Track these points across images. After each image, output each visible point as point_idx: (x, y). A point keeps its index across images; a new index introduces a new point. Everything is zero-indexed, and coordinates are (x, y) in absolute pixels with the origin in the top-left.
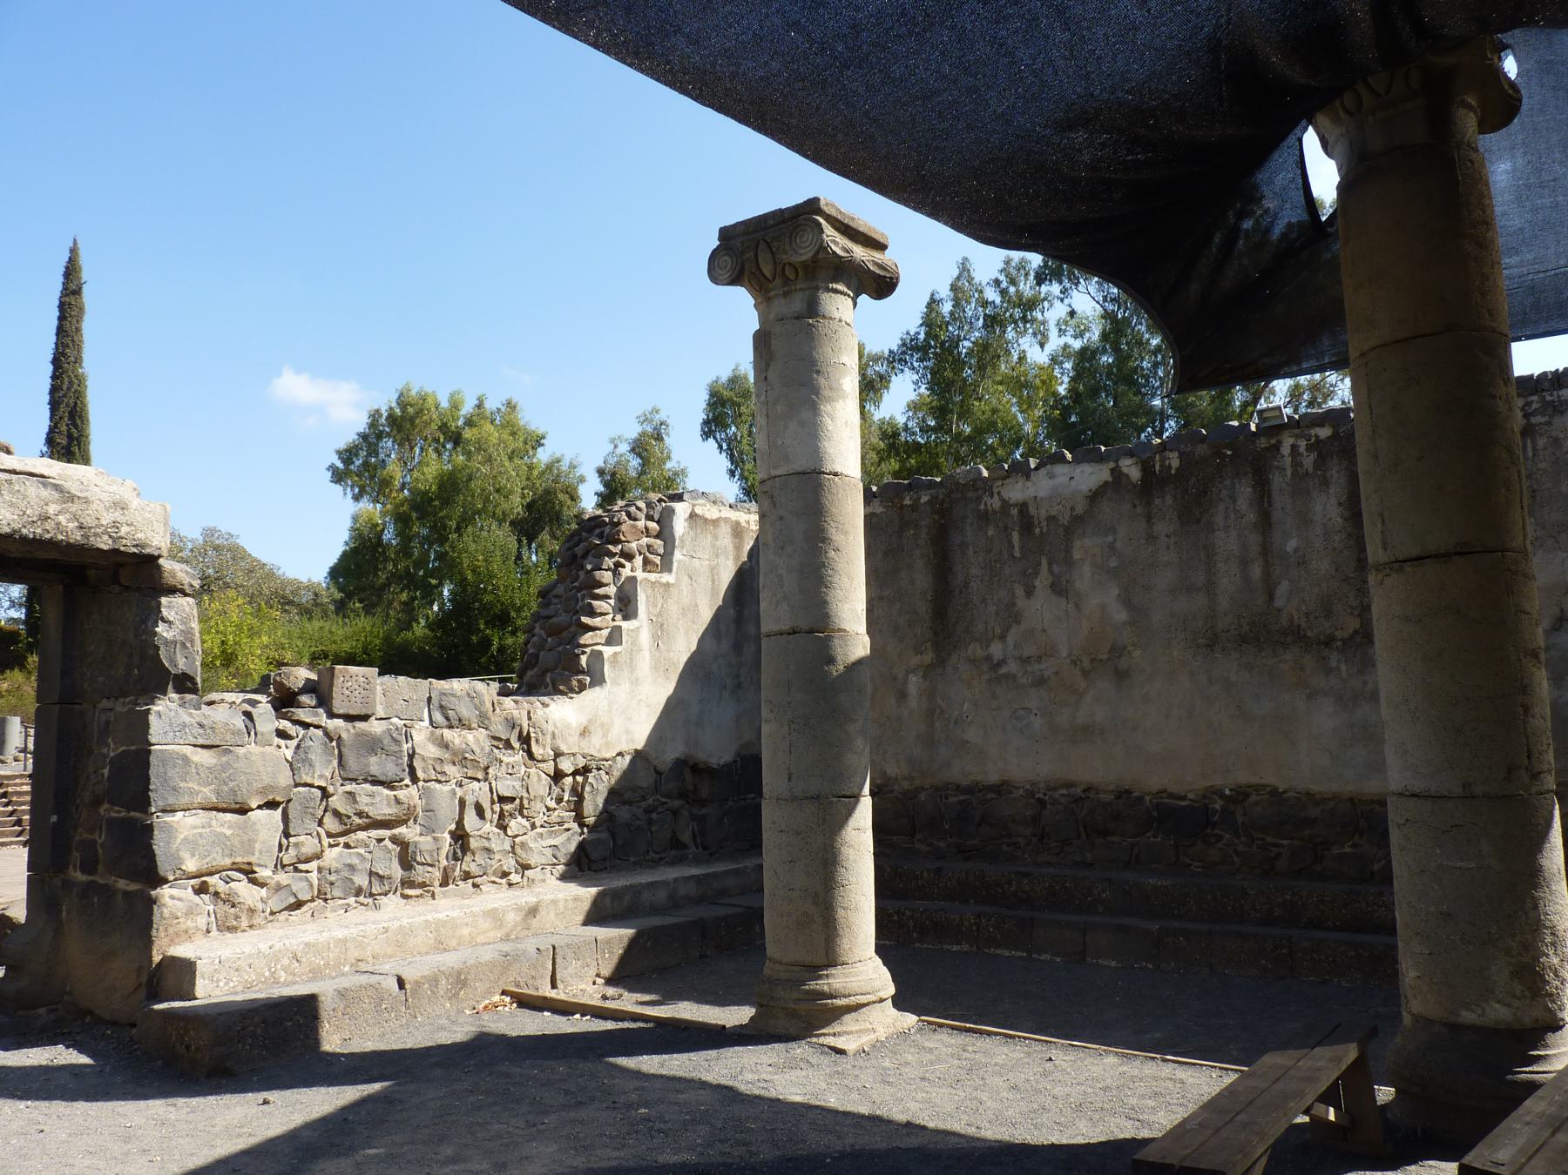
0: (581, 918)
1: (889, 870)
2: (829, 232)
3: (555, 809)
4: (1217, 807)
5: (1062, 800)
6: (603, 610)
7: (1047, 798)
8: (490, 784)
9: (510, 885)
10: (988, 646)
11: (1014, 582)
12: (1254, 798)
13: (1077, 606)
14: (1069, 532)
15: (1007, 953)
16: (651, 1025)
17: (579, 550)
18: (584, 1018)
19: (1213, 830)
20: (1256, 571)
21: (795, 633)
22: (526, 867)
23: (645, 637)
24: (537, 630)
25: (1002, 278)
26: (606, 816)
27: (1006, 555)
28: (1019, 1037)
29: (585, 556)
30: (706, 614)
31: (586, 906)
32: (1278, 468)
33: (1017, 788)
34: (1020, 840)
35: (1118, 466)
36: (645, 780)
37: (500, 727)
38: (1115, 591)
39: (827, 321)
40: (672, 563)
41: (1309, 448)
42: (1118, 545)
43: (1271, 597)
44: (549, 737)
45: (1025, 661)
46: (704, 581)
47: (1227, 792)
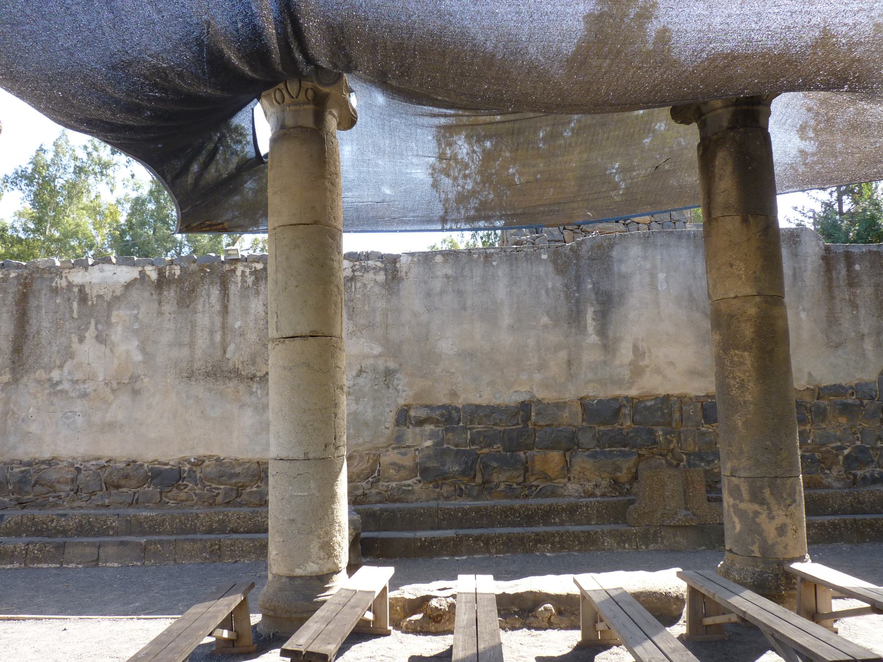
4: (186, 468)
5: (92, 468)
7: (82, 467)
10: (50, 372)
11: (72, 333)
12: (207, 463)
13: (112, 350)
14: (109, 304)
15: (45, 566)
19: (183, 482)
20: (218, 337)
27: (67, 316)
28: (45, 619)
32: (234, 282)
33: (63, 461)
34: (62, 494)
35: (144, 270)
38: (136, 343)
41: (251, 273)
42: (140, 316)
43: (225, 352)
47: (192, 460)
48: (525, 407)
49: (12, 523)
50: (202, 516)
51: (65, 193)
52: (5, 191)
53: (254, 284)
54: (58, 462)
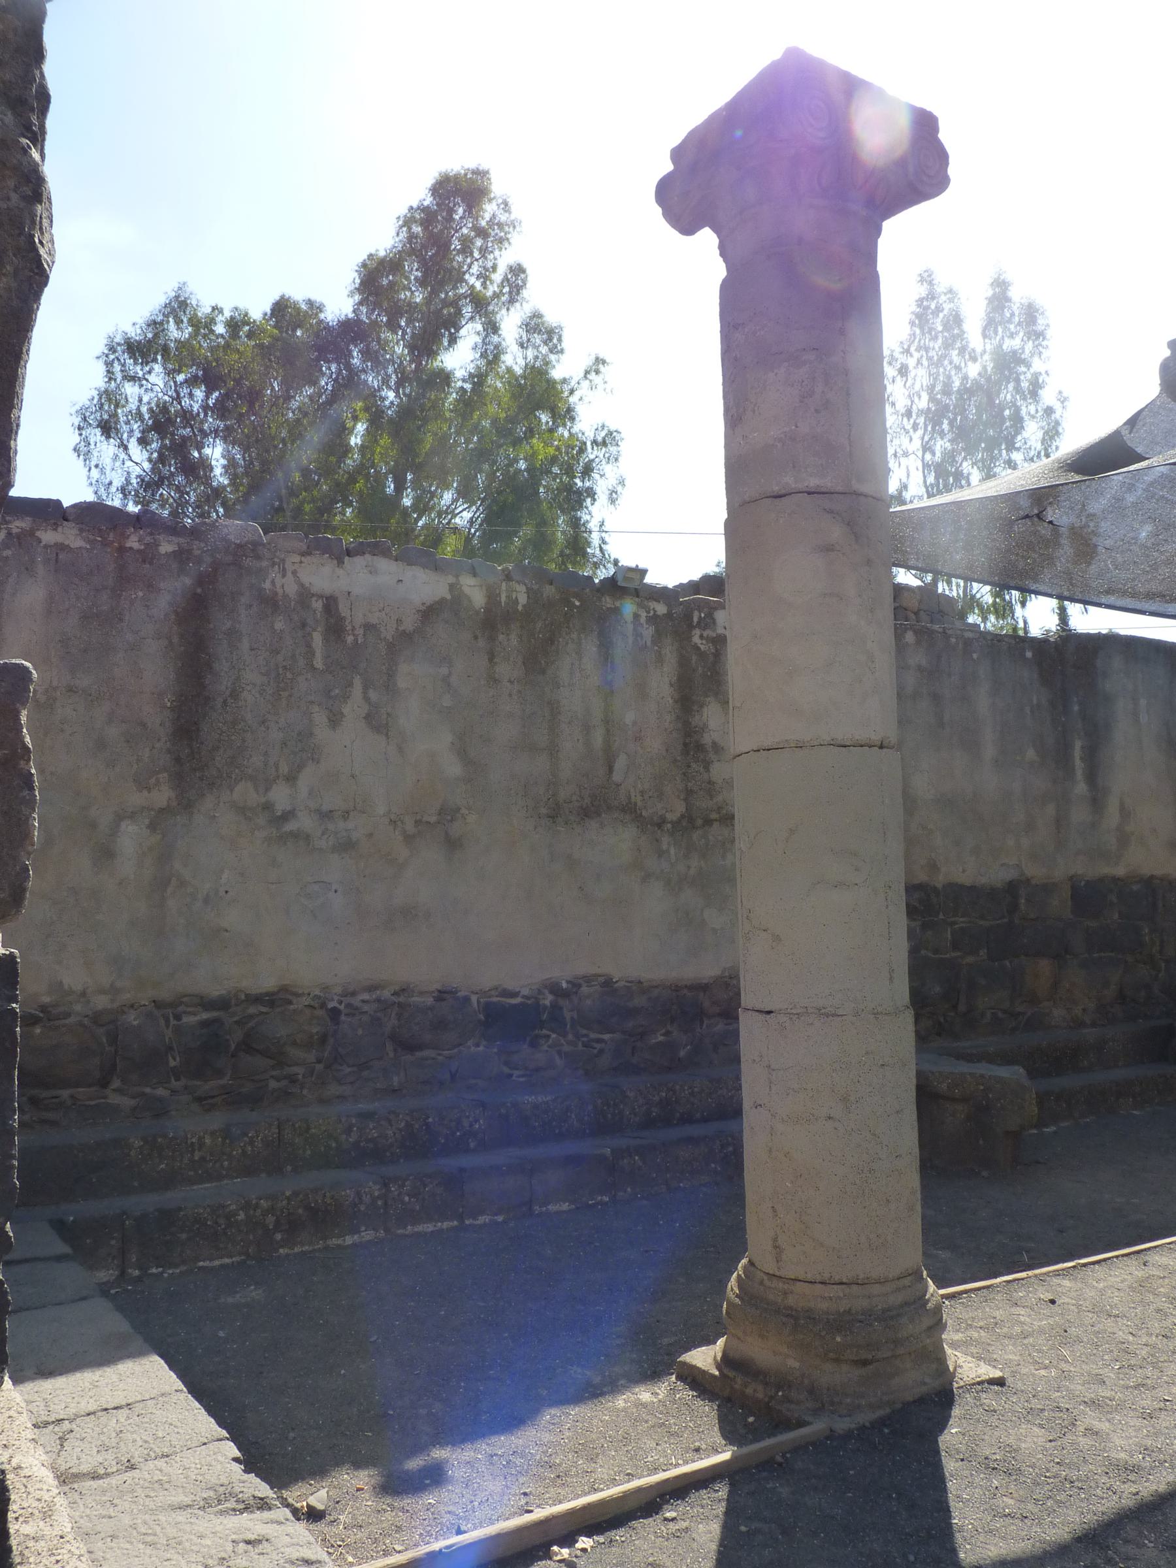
1: (138, 1143)
4: (547, 1002)
5: (366, 1008)
7: (342, 1007)
10: (267, 790)
11: (312, 702)
12: (585, 989)
13: (400, 750)
14: (393, 649)
15: (429, 1227)
27: (301, 662)
34: (295, 1069)
43: (611, 769)
45: (326, 816)
47: (564, 985)
48: (1012, 887)
49: (259, 1144)
53: (654, 642)
54: (290, 997)
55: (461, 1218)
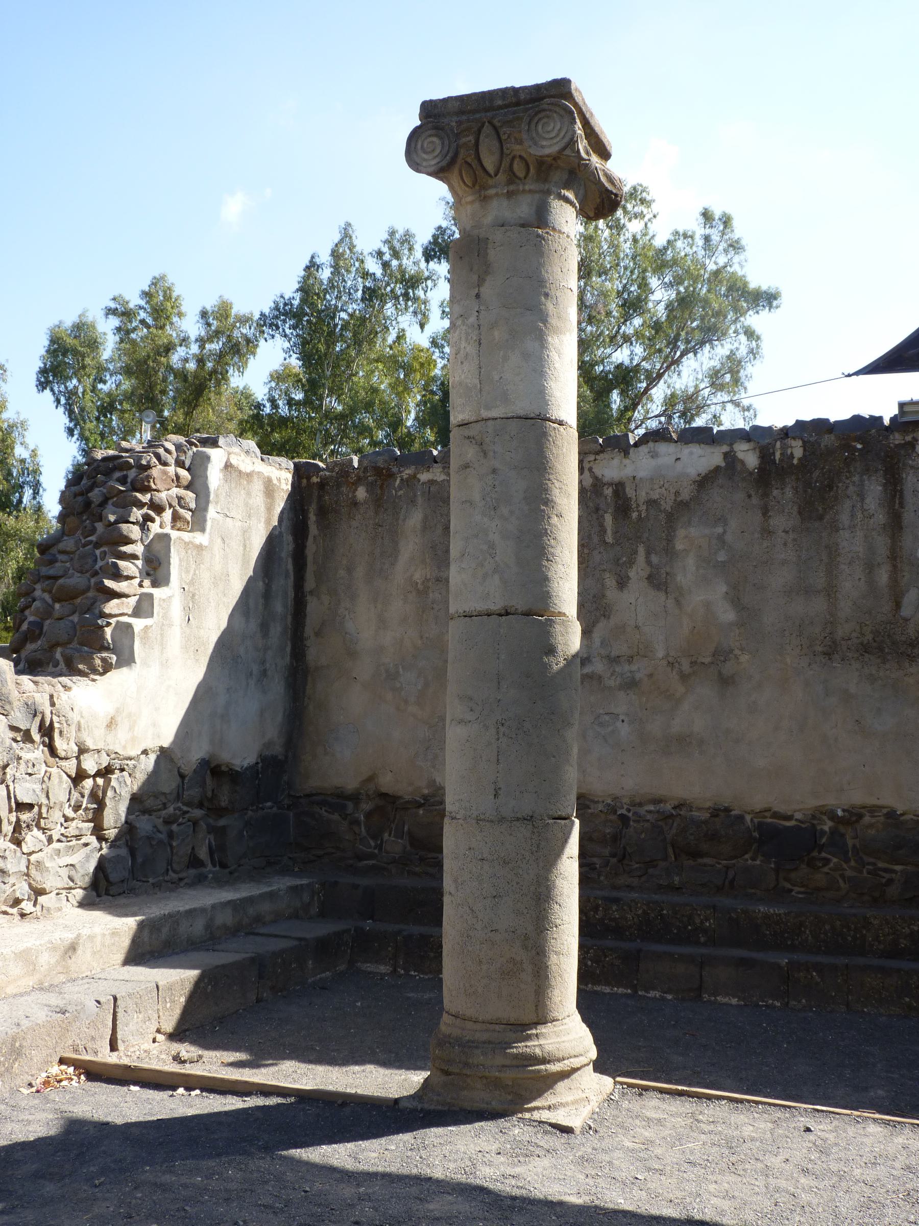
0: (120, 957)
2: (579, 124)
3: (73, 819)
4: (826, 828)
5: (649, 817)
6: (130, 573)
7: (630, 815)
8: (7, 786)
9: (23, 915)
11: (604, 570)
12: (867, 819)
13: (678, 602)
14: (671, 518)
15: (607, 990)
16: (293, 1099)
17: (95, 495)
18: (193, 1093)
19: (820, 853)
20: (883, 577)
21: (507, 614)
22: (39, 892)
23: (176, 611)
24: (38, 593)
25: (385, 249)
26: (128, 829)
27: (596, 539)
28: (749, 1101)
29: (103, 504)
30: (237, 587)
31: (126, 942)
32: (912, 467)
33: (598, 802)
34: (595, 860)
35: (732, 450)
36: (169, 785)
37: (18, 714)
38: (723, 588)
39: (557, 235)
40: (205, 521)
42: (729, 538)
43: (898, 605)
44: (73, 728)
45: (614, 660)
46: (235, 545)
47: (840, 813)
50: (876, 922)
51: (349, 334)
52: (262, 342)
54: (588, 803)
55: (635, 988)
